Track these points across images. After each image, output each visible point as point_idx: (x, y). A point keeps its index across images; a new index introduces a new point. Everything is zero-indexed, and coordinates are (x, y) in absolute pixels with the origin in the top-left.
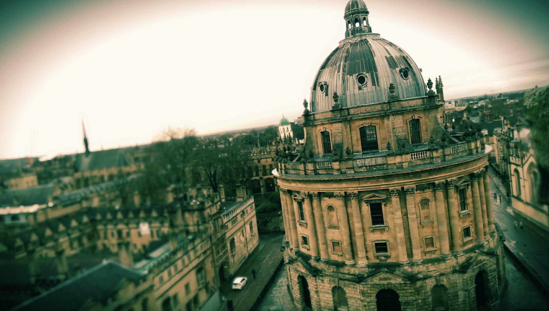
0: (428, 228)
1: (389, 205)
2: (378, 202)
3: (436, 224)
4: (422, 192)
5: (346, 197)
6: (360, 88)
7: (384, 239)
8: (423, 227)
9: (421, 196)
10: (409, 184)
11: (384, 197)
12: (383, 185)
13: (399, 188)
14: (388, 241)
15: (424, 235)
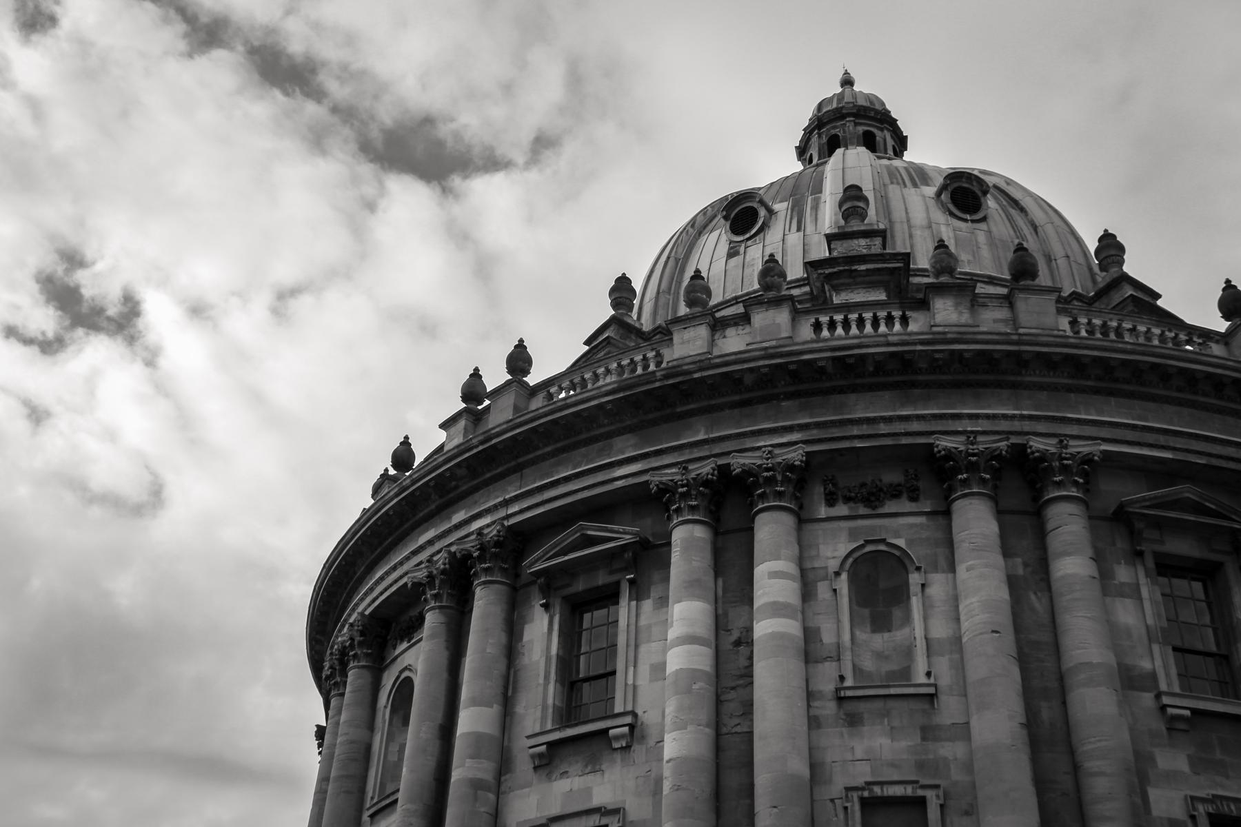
0: (893, 733)
1: (655, 592)
2: (602, 578)
3: (949, 711)
4: (862, 510)
5: (458, 580)
6: (732, 253)
7: (596, 802)
8: (853, 721)
9: (853, 535)
10: (772, 441)
11: (622, 533)
12: (625, 464)
13: (706, 469)
14: (616, 811)
15: (861, 774)
